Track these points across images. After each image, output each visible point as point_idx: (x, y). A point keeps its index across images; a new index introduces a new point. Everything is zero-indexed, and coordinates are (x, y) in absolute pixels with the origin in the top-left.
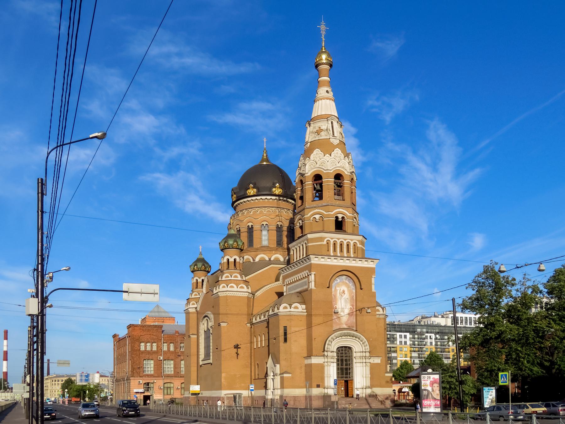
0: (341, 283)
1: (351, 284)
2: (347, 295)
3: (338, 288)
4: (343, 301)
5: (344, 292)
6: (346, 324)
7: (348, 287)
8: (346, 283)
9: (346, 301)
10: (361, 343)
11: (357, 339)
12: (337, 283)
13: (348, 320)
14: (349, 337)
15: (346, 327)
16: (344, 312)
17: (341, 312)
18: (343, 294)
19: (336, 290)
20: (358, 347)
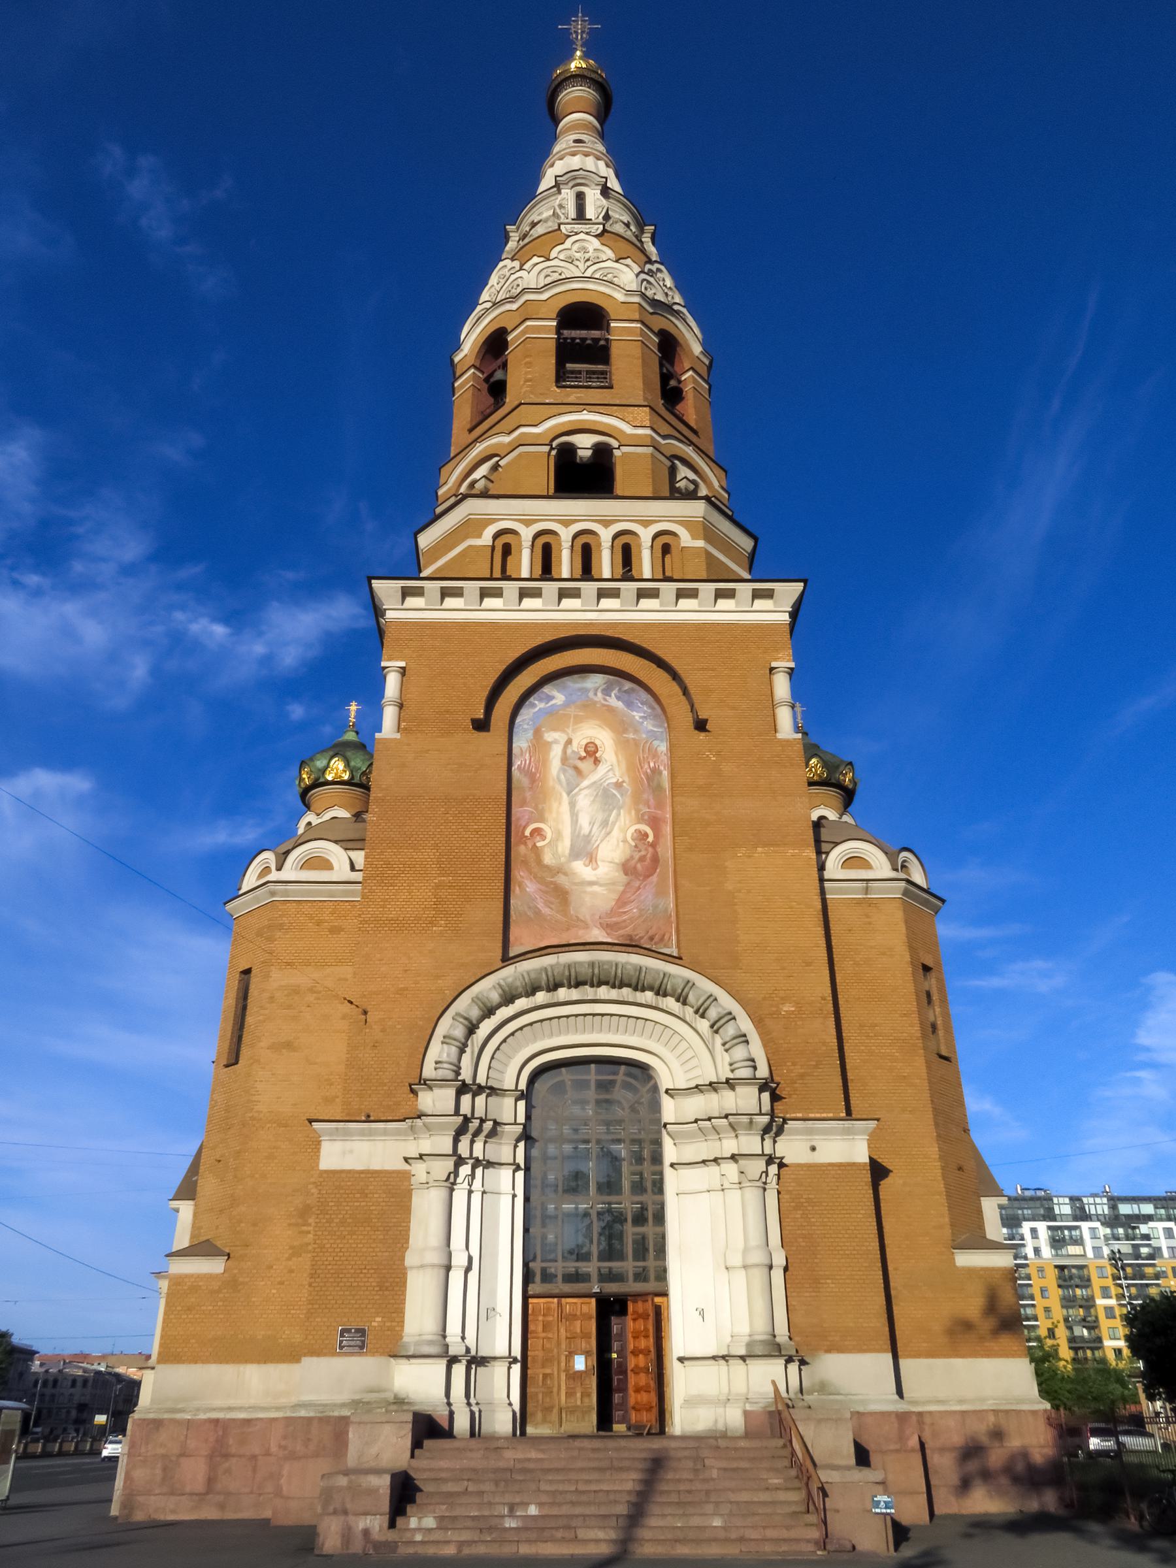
0: (572, 711)
1: (640, 715)
2: (611, 767)
3: (554, 737)
4: (584, 800)
5: (592, 752)
6: (608, 927)
7: (620, 726)
8: (611, 709)
9: (606, 797)
10: (704, 1025)
11: (670, 1003)
12: (551, 713)
13: (621, 902)
14: (603, 992)
15: (598, 935)
16: (591, 859)
17: (575, 854)
18: (585, 766)
19: (539, 746)
20: (686, 1056)
